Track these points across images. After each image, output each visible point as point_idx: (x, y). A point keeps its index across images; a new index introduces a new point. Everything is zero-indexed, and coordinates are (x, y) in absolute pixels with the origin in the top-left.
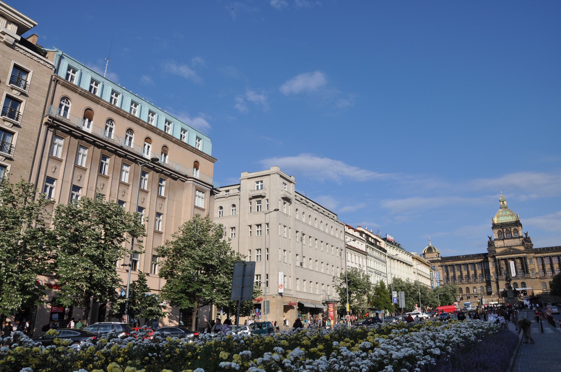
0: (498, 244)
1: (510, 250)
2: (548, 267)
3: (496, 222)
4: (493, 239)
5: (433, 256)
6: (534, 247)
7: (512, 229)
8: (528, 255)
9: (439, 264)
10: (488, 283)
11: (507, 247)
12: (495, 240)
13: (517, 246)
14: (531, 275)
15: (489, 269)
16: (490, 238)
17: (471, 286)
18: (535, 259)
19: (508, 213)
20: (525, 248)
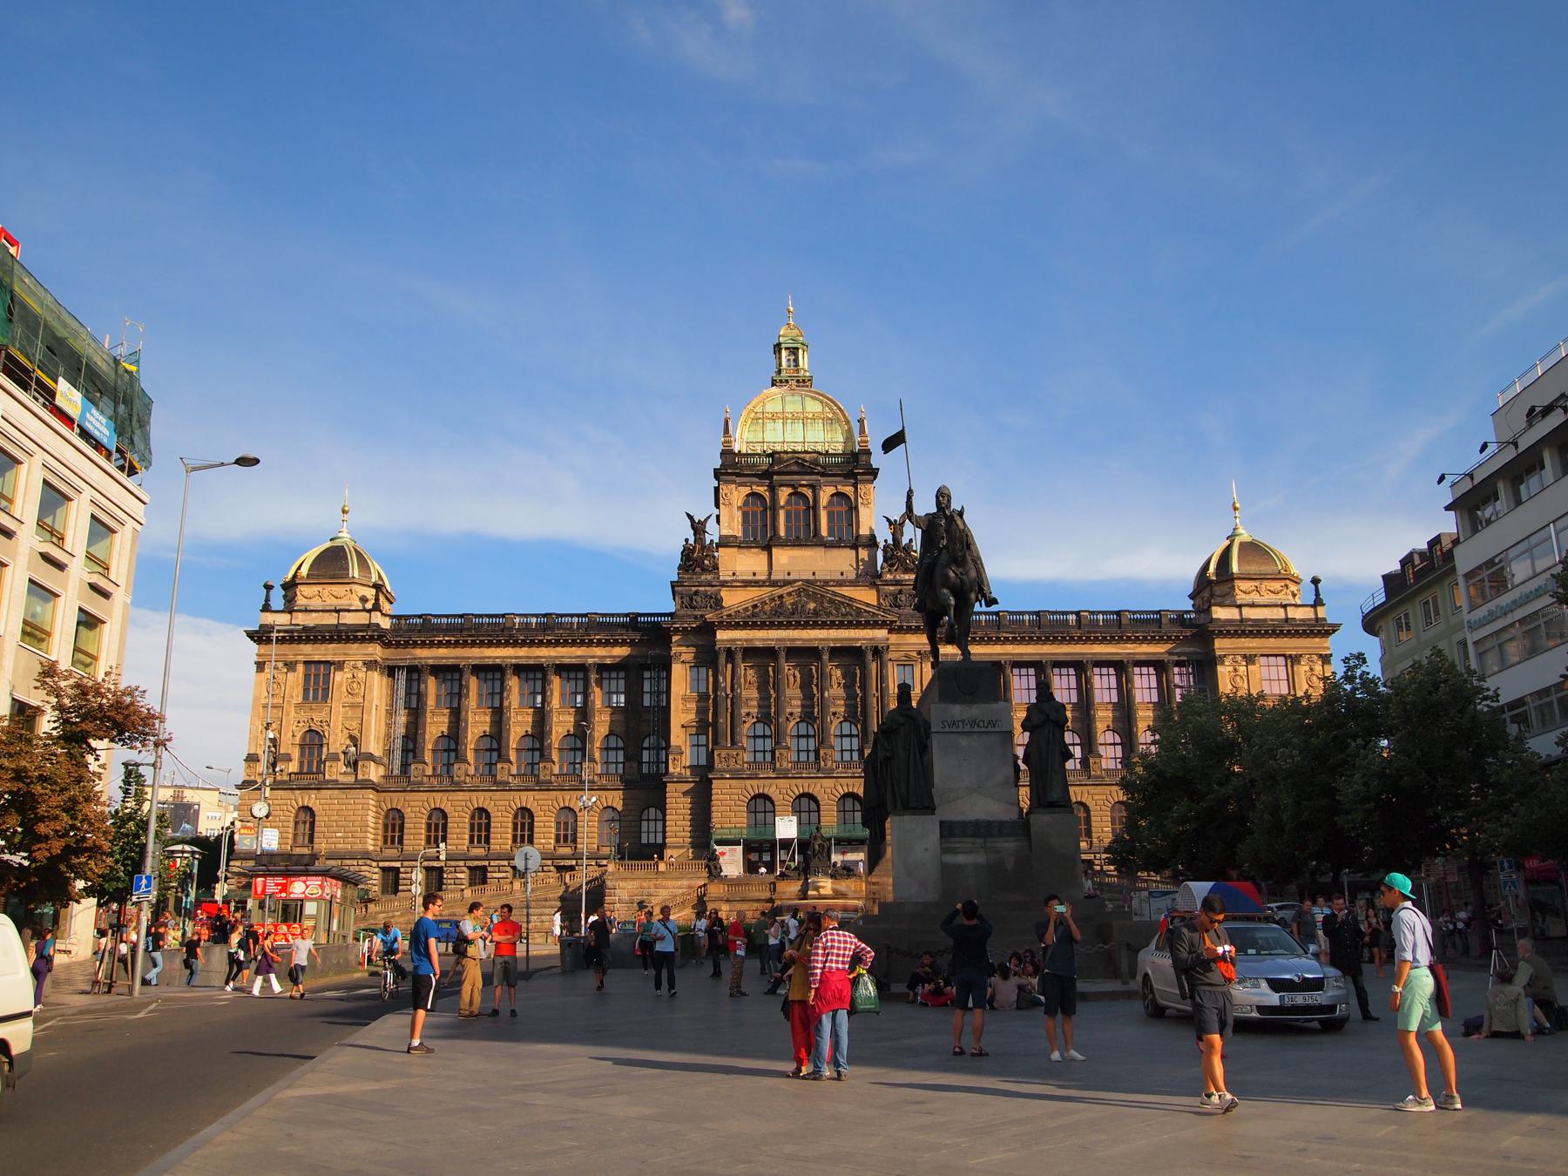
7: (825, 494)
8: (894, 638)
9: (376, 651)
12: (725, 542)
13: (840, 583)
15: (666, 711)
16: (698, 528)
17: (545, 807)
19: (813, 407)
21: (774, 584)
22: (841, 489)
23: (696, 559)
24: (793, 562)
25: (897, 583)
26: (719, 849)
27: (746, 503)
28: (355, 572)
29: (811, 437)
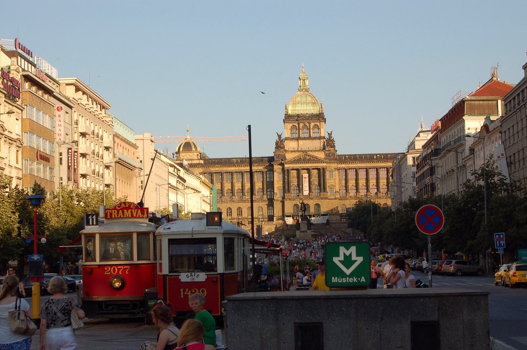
0: (290, 145)
1: (305, 157)
2: (352, 183)
3: (290, 112)
4: (283, 137)
5: (192, 157)
6: (339, 153)
7: (312, 124)
8: (328, 165)
10: (271, 203)
11: (302, 151)
12: (286, 139)
13: (315, 151)
14: (329, 194)
15: (273, 182)
16: (280, 136)
18: (337, 172)
19: (309, 99)
20: (326, 155)
21: (298, 151)
22: (316, 123)
23: (279, 145)
24: (304, 145)
25: (329, 151)
26: (286, 218)
27: (291, 127)
28: (194, 149)
29: (308, 108)
